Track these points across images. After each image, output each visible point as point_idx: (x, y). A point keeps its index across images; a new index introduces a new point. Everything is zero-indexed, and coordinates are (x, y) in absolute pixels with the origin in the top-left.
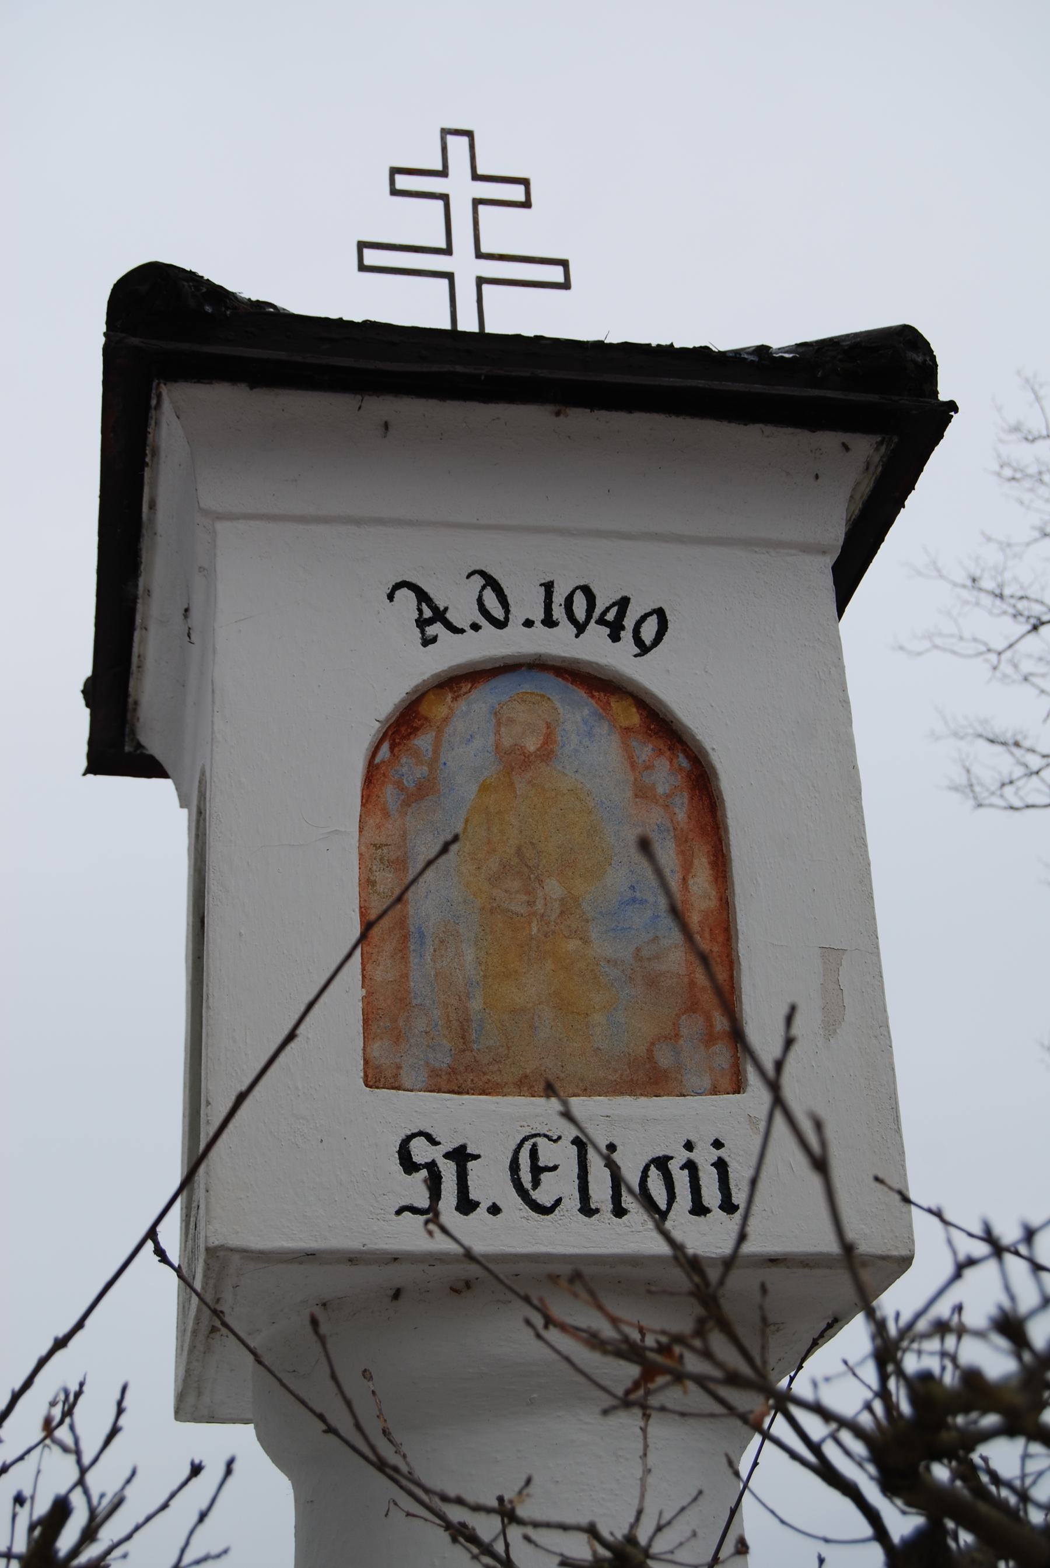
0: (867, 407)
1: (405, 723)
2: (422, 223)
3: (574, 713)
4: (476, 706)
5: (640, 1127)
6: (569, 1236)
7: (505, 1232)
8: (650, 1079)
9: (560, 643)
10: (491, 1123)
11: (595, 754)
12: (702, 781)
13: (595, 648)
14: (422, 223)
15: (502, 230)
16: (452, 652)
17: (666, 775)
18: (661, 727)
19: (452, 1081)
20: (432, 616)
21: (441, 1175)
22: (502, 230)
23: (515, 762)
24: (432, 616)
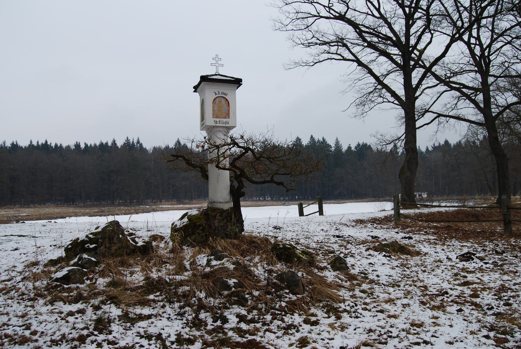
0: (237, 82)
1: (214, 100)
2: (214, 62)
3: (223, 99)
4: (218, 99)
6: (221, 125)
7: (218, 125)
8: (225, 118)
9: (222, 95)
10: (218, 120)
11: (223, 101)
12: (228, 103)
13: (224, 96)
14: (214, 62)
15: (220, 62)
16: (217, 96)
17: (227, 102)
18: (227, 100)
19: (216, 118)
20: (216, 94)
21: (216, 122)
22: (220, 62)
23: (220, 102)
24: (216, 94)
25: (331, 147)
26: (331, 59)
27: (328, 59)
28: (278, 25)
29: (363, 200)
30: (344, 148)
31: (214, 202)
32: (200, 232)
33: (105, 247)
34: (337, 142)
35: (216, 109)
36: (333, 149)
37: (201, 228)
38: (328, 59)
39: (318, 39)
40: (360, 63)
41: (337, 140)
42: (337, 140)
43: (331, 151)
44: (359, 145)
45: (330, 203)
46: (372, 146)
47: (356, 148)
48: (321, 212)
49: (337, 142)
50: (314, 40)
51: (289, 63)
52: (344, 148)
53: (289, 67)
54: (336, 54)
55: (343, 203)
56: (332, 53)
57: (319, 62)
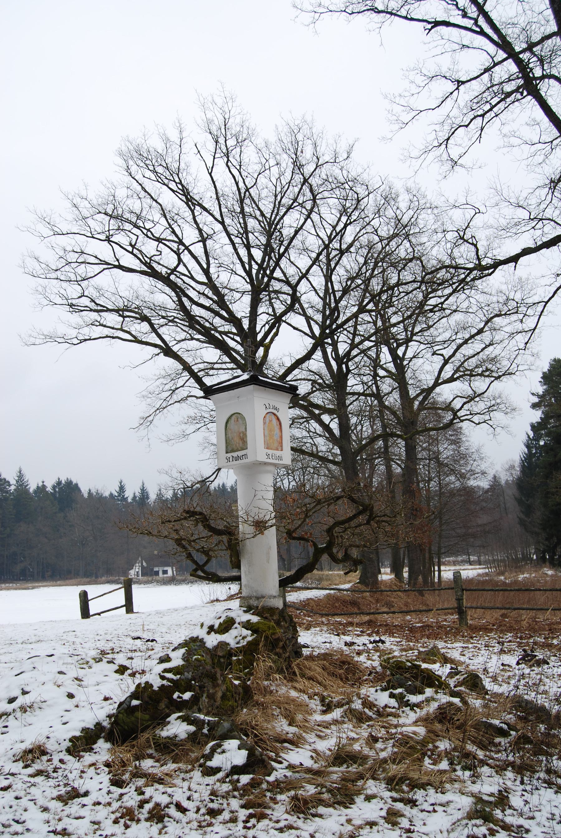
3: (273, 417)
5: (278, 453)
8: (277, 449)
10: (270, 452)
11: (274, 421)
18: (278, 419)
19: (268, 448)
21: (268, 455)
23: (271, 421)
25: (10, 485)
26: (113, 338)
27: (107, 337)
28: (32, 264)
29: (68, 582)
30: (32, 487)
31: (263, 597)
32: (281, 651)
33: (208, 696)
34: (20, 476)
35: (266, 433)
36: (13, 488)
37: (281, 644)
38: (107, 337)
39: (93, 301)
40: (168, 351)
41: (20, 472)
42: (20, 472)
43: (7, 492)
44: (59, 483)
45: (8, 589)
46: (80, 485)
47: (54, 487)
48: (129, 606)
49: (20, 476)
50: (85, 301)
51: (35, 334)
52: (32, 487)
53: (32, 340)
54: (121, 330)
55: (33, 588)
56: (113, 328)
57: (90, 339)
